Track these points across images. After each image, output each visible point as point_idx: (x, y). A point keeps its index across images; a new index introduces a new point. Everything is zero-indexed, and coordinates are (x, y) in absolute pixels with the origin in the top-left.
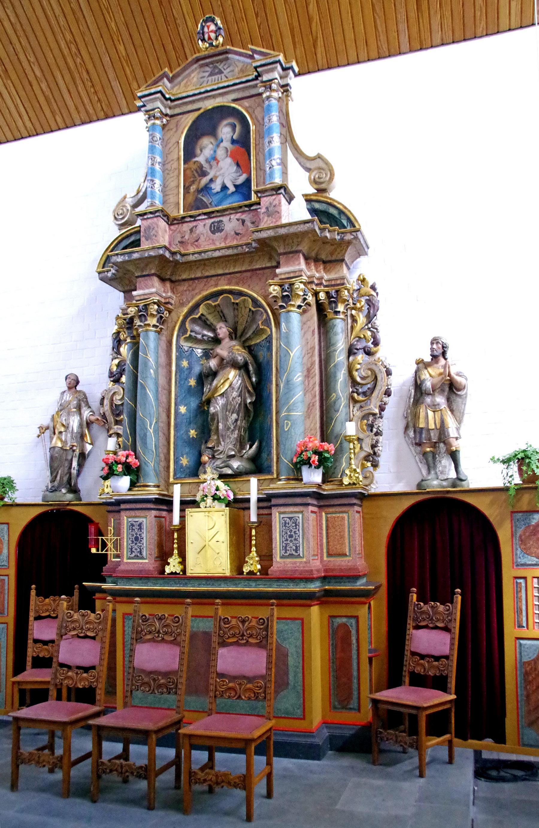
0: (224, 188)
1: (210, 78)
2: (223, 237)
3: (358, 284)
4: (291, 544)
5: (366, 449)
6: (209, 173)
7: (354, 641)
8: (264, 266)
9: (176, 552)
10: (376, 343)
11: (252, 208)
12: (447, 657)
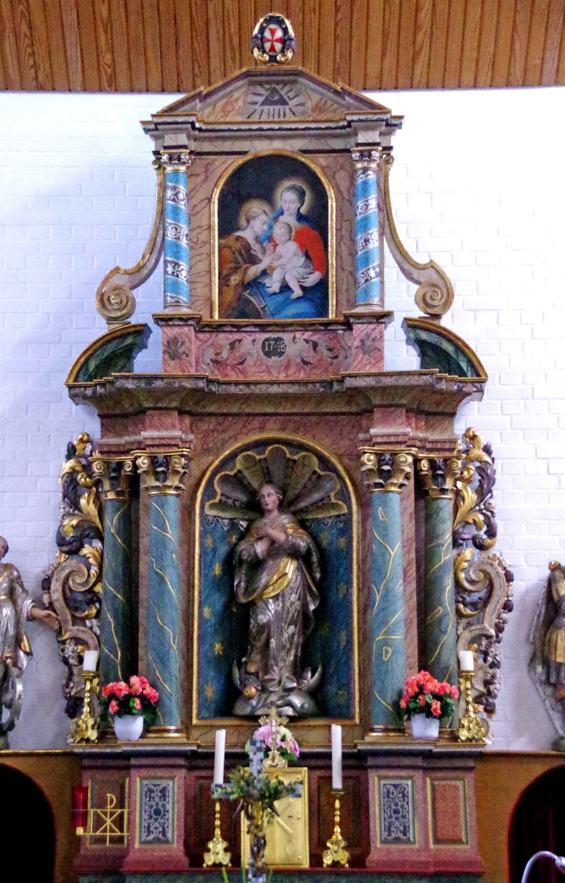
0: (285, 288)
1: (266, 108)
2: (284, 364)
3: (466, 443)
4: (397, 824)
6: (261, 261)
8: (338, 410)
9: (218, 832)
11: (330, 328)
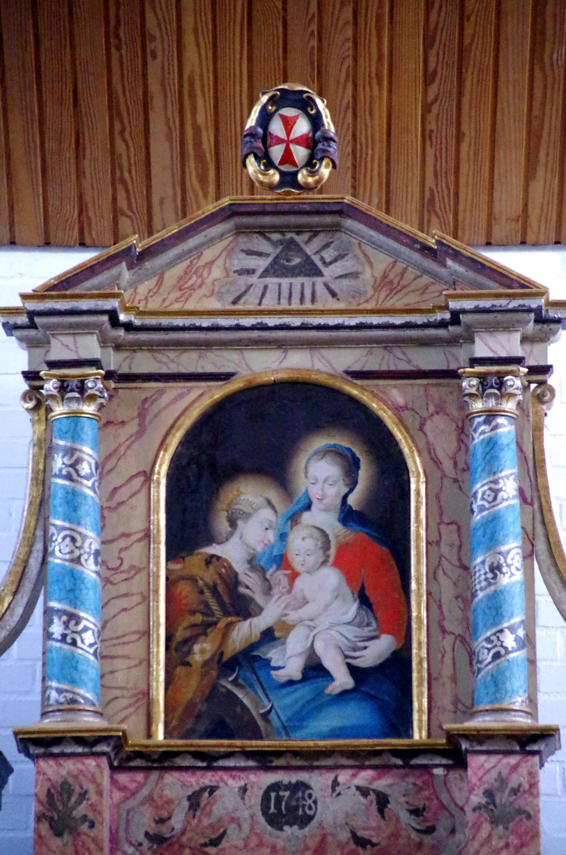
0: (315, 670)
1: (272, 281)
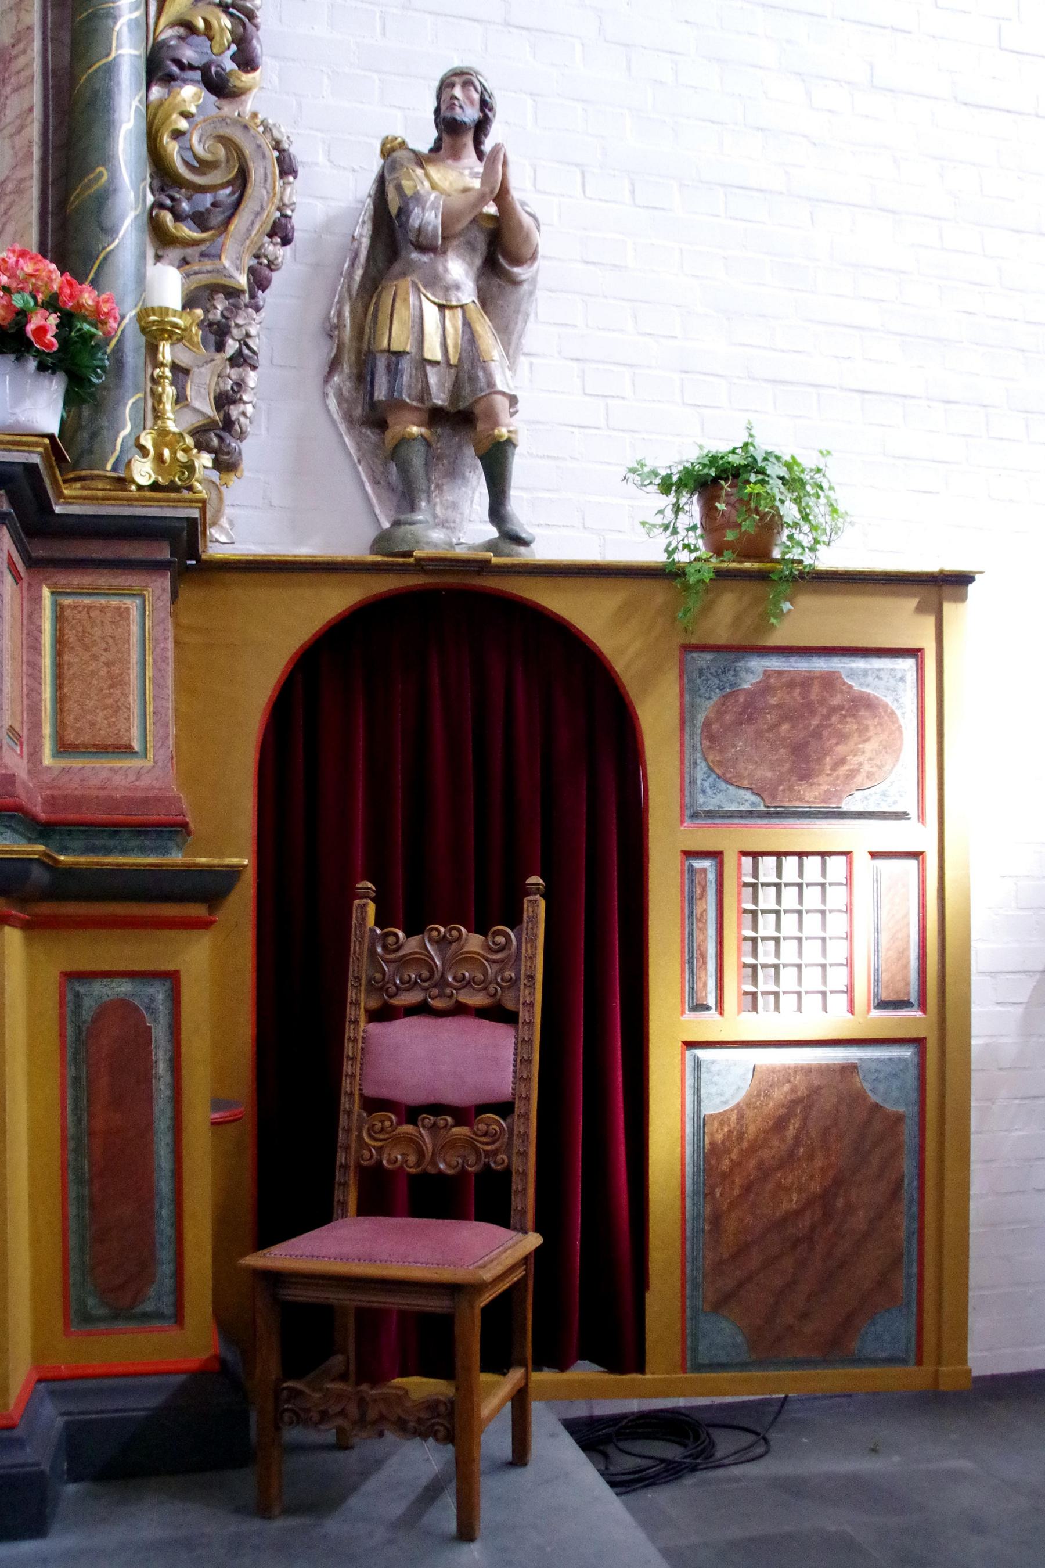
5: (197, 404)
7: (162, 1068)
10: (247, 62)
12: (504, 1109)
